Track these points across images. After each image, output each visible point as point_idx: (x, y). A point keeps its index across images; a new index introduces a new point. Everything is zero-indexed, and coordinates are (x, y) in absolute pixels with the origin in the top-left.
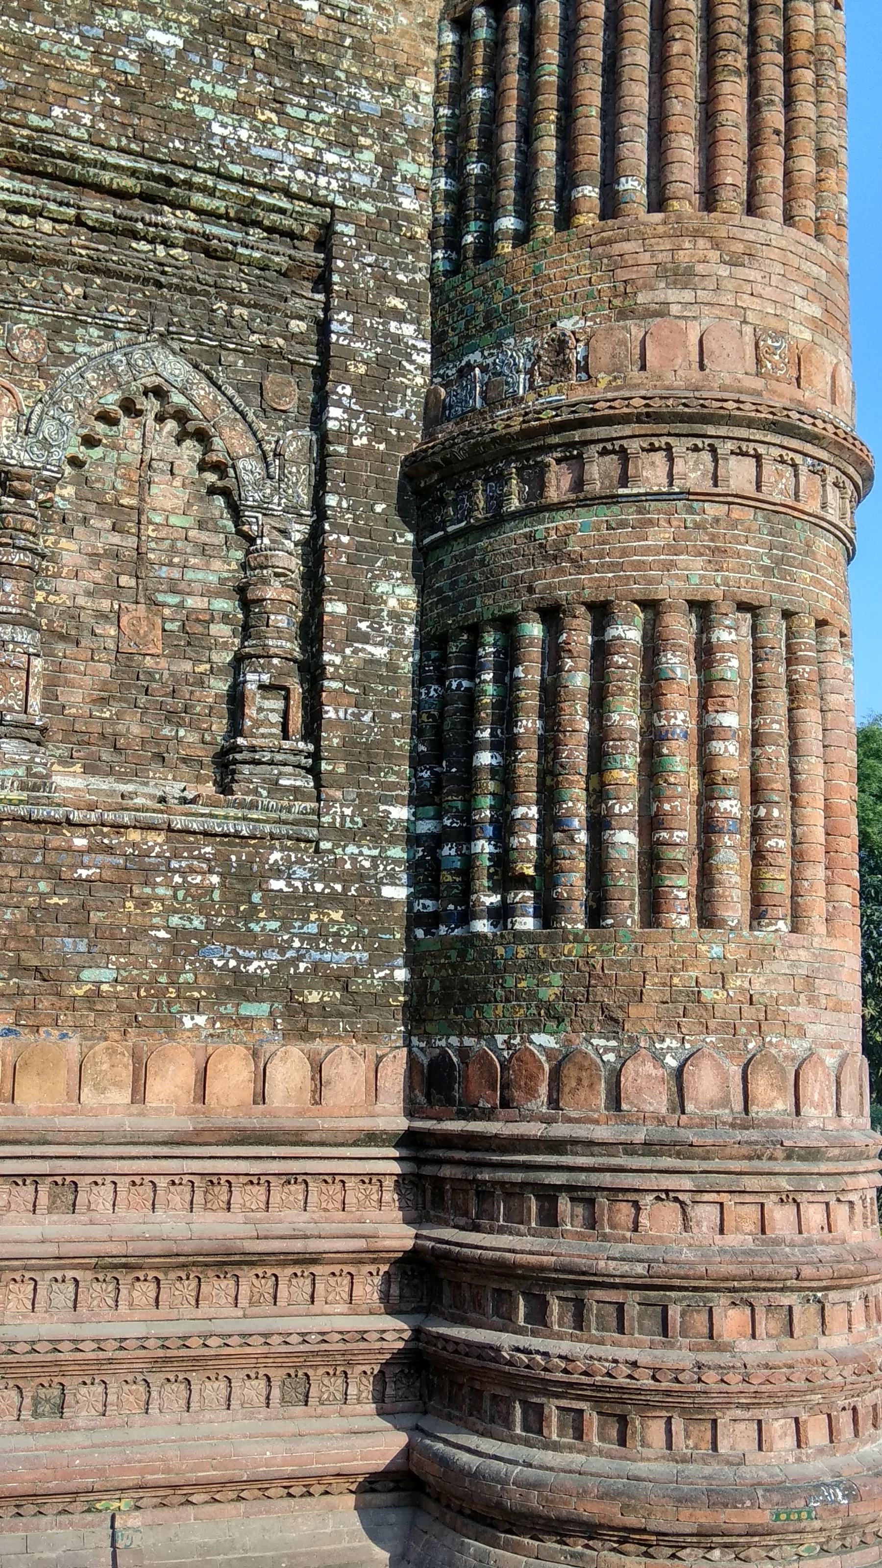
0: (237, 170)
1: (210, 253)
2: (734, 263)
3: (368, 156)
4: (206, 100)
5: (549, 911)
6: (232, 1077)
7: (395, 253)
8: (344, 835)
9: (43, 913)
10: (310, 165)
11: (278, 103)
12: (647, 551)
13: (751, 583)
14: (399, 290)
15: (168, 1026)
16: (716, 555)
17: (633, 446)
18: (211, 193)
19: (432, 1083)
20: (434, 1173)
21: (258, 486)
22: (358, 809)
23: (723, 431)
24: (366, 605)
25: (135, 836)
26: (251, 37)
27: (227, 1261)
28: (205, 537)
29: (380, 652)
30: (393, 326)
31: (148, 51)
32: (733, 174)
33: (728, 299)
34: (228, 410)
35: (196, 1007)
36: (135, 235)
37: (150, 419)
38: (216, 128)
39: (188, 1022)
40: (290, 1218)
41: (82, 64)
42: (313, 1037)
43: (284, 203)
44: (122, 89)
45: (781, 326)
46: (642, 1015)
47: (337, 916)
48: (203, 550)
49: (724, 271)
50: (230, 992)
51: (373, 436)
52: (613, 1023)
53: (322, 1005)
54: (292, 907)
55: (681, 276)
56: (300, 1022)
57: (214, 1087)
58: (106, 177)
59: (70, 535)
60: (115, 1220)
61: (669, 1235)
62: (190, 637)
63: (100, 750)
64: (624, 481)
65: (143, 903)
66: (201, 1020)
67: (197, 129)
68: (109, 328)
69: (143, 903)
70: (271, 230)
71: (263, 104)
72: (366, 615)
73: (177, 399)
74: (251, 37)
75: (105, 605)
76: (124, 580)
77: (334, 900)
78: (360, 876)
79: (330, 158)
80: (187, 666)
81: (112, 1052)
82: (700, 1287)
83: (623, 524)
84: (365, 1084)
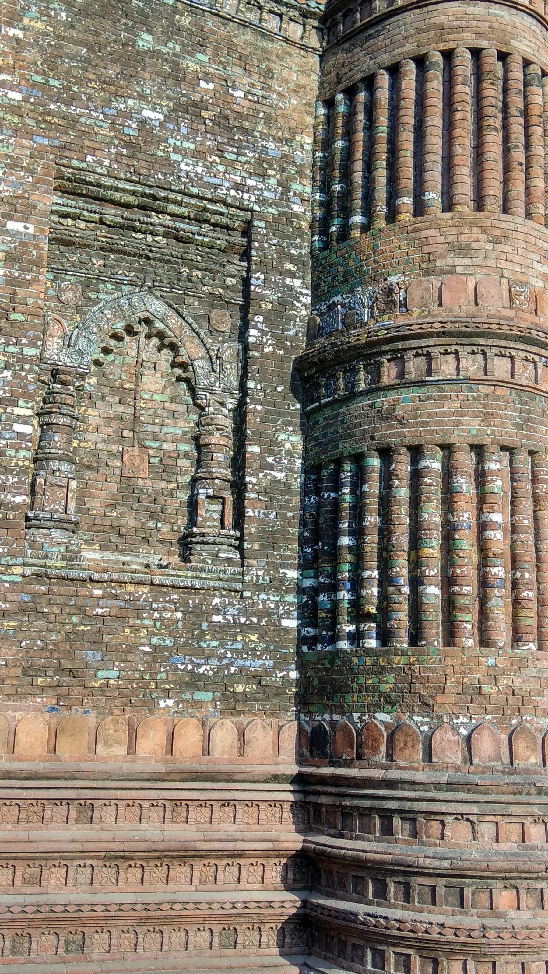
0: (195, 191)
1: (178, 239)
2: (496, 241)
3: (273, 181)
4: (177, 150)
5: (385, 636)
6: (189, 739)
7: (289, 238)
8: (259, 588)
9: (73, 636)
10: (238, 187)
11: (220, 151)
12: (444, 414)
13: (508, 434)
14: (291, 259)
15: (150, 706)
16: (487, 417)
17: (435, 351)
18: (179, 204)
19: (314, 743)
20: (315, 800)
21: (207, 376)
22: (267, 571)
23: (490, 342)
24: (272, 447)
25: (131, 588)
26: (204, 113)
27: (185, 855)
28: (174, 407)
29: (280, 476)
30: (288, 281)
31: (143, 122)
32: (494, 188)
33: (492, 263)
34: (188, 331)
35: (167, 694)
36: (134, 229)
37: (142, 339)
38: (183, 166)
39: (162, 704)
40: (225, 828)
41: (105, 131)
42: (239, 713)
43: (223, 209)
44: (128, 144)
45: (525, 279)
46: (444, 702)
47: (254, 638)
48: (173, 414)
49: (489, 246)
50: (188, 685)
51: (276, 346)
52: (427, 707)
53: (244, 694)
54: (226, 632)
55: (463, 250)
56: (232, 704)
57: (178, 744)
58: (117, 196)
59: (94, 406)
60: (117, 828)
61: (462, 842)
62: (165, 467)
63: (110, 536)
64: (429, 372)
65: (136, 629)
66: (170, 702)
68: (118, 284)
69: (136, 629)
70: (215, 225)
71: (210, 153)
72: (271, 453)
73: (159, 325)
74: (204, 113)
75: (114, 448)
76: (126, 433)
77: (252, 628)
78: (268, 613)
79: (251, 182)
80: (163, 484)
81: (116, 722)
82: (484, 876)
83: (429, 398)
84: (271, 743)
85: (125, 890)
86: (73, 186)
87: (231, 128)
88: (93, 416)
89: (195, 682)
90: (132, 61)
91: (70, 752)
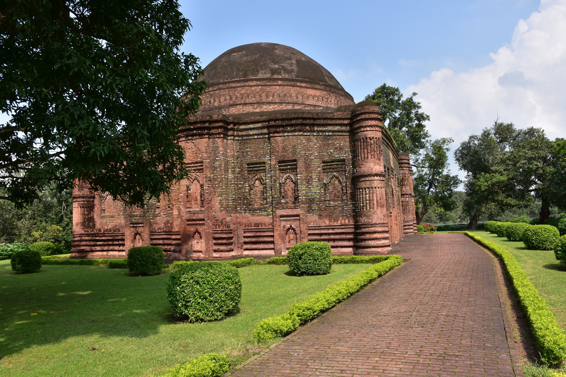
13: (368, 186)
55: (362, 164)
63: (334, 201)
67: (334, 157)
84: (352, 222)
85: (337, 237)
86: (323, 163)
87: (341, 149)
88: (330, 187)
89: (343, 216)
90: (329, 145)
91: (331, 224)
